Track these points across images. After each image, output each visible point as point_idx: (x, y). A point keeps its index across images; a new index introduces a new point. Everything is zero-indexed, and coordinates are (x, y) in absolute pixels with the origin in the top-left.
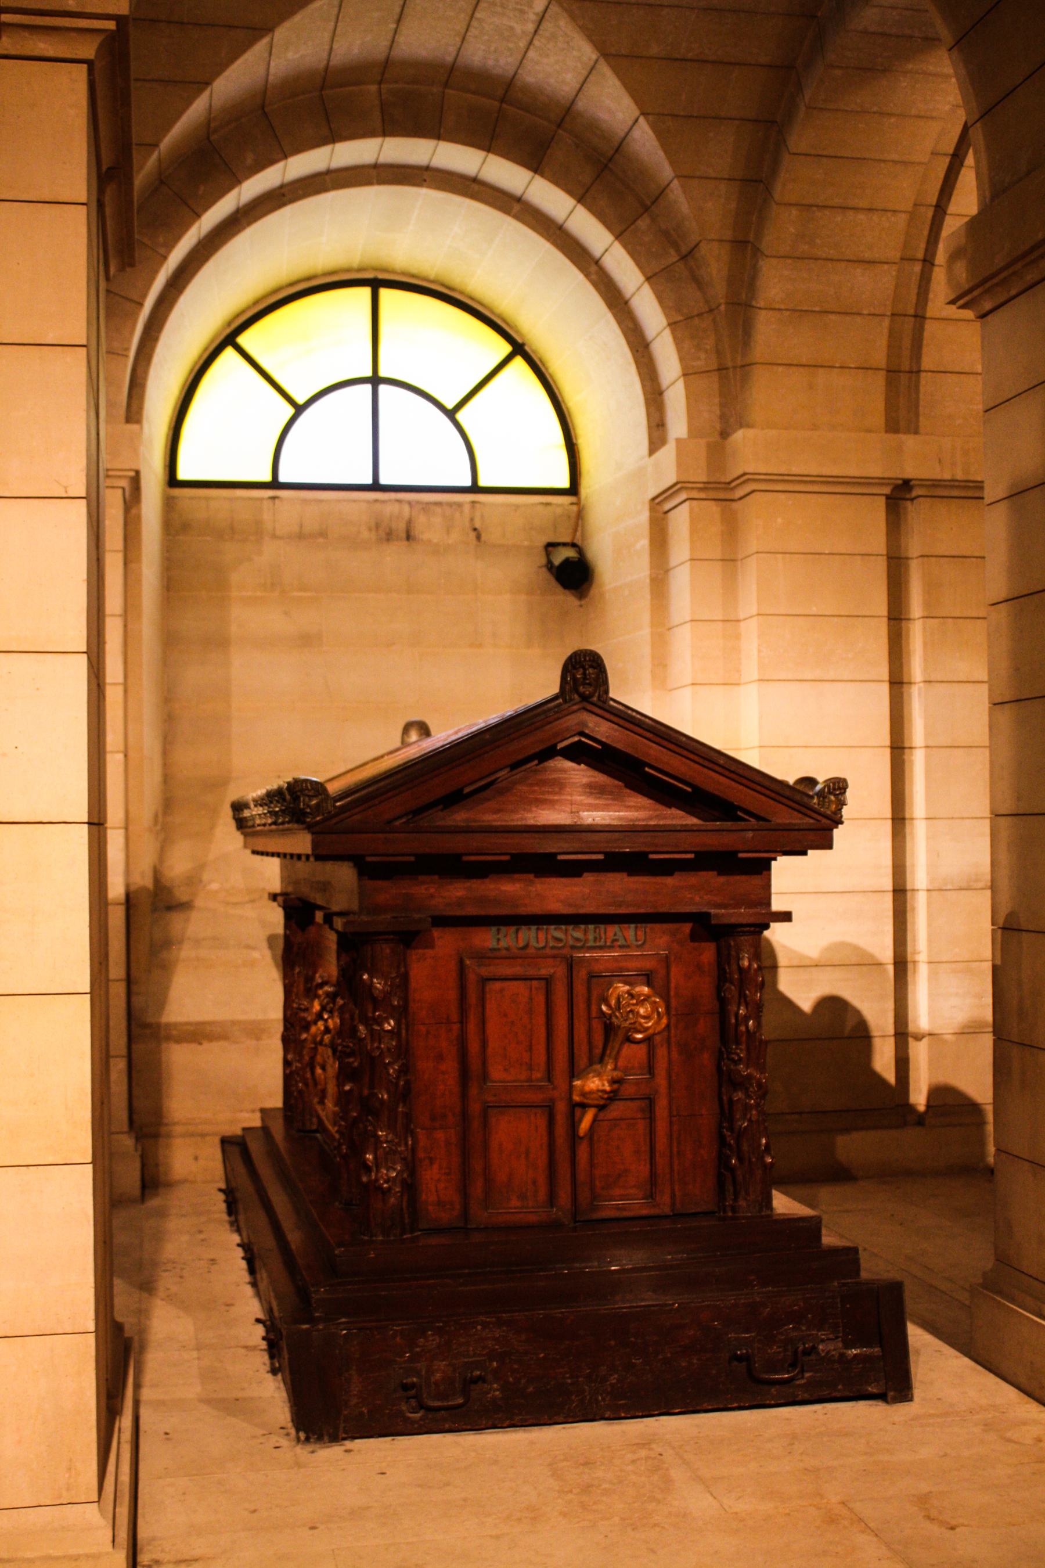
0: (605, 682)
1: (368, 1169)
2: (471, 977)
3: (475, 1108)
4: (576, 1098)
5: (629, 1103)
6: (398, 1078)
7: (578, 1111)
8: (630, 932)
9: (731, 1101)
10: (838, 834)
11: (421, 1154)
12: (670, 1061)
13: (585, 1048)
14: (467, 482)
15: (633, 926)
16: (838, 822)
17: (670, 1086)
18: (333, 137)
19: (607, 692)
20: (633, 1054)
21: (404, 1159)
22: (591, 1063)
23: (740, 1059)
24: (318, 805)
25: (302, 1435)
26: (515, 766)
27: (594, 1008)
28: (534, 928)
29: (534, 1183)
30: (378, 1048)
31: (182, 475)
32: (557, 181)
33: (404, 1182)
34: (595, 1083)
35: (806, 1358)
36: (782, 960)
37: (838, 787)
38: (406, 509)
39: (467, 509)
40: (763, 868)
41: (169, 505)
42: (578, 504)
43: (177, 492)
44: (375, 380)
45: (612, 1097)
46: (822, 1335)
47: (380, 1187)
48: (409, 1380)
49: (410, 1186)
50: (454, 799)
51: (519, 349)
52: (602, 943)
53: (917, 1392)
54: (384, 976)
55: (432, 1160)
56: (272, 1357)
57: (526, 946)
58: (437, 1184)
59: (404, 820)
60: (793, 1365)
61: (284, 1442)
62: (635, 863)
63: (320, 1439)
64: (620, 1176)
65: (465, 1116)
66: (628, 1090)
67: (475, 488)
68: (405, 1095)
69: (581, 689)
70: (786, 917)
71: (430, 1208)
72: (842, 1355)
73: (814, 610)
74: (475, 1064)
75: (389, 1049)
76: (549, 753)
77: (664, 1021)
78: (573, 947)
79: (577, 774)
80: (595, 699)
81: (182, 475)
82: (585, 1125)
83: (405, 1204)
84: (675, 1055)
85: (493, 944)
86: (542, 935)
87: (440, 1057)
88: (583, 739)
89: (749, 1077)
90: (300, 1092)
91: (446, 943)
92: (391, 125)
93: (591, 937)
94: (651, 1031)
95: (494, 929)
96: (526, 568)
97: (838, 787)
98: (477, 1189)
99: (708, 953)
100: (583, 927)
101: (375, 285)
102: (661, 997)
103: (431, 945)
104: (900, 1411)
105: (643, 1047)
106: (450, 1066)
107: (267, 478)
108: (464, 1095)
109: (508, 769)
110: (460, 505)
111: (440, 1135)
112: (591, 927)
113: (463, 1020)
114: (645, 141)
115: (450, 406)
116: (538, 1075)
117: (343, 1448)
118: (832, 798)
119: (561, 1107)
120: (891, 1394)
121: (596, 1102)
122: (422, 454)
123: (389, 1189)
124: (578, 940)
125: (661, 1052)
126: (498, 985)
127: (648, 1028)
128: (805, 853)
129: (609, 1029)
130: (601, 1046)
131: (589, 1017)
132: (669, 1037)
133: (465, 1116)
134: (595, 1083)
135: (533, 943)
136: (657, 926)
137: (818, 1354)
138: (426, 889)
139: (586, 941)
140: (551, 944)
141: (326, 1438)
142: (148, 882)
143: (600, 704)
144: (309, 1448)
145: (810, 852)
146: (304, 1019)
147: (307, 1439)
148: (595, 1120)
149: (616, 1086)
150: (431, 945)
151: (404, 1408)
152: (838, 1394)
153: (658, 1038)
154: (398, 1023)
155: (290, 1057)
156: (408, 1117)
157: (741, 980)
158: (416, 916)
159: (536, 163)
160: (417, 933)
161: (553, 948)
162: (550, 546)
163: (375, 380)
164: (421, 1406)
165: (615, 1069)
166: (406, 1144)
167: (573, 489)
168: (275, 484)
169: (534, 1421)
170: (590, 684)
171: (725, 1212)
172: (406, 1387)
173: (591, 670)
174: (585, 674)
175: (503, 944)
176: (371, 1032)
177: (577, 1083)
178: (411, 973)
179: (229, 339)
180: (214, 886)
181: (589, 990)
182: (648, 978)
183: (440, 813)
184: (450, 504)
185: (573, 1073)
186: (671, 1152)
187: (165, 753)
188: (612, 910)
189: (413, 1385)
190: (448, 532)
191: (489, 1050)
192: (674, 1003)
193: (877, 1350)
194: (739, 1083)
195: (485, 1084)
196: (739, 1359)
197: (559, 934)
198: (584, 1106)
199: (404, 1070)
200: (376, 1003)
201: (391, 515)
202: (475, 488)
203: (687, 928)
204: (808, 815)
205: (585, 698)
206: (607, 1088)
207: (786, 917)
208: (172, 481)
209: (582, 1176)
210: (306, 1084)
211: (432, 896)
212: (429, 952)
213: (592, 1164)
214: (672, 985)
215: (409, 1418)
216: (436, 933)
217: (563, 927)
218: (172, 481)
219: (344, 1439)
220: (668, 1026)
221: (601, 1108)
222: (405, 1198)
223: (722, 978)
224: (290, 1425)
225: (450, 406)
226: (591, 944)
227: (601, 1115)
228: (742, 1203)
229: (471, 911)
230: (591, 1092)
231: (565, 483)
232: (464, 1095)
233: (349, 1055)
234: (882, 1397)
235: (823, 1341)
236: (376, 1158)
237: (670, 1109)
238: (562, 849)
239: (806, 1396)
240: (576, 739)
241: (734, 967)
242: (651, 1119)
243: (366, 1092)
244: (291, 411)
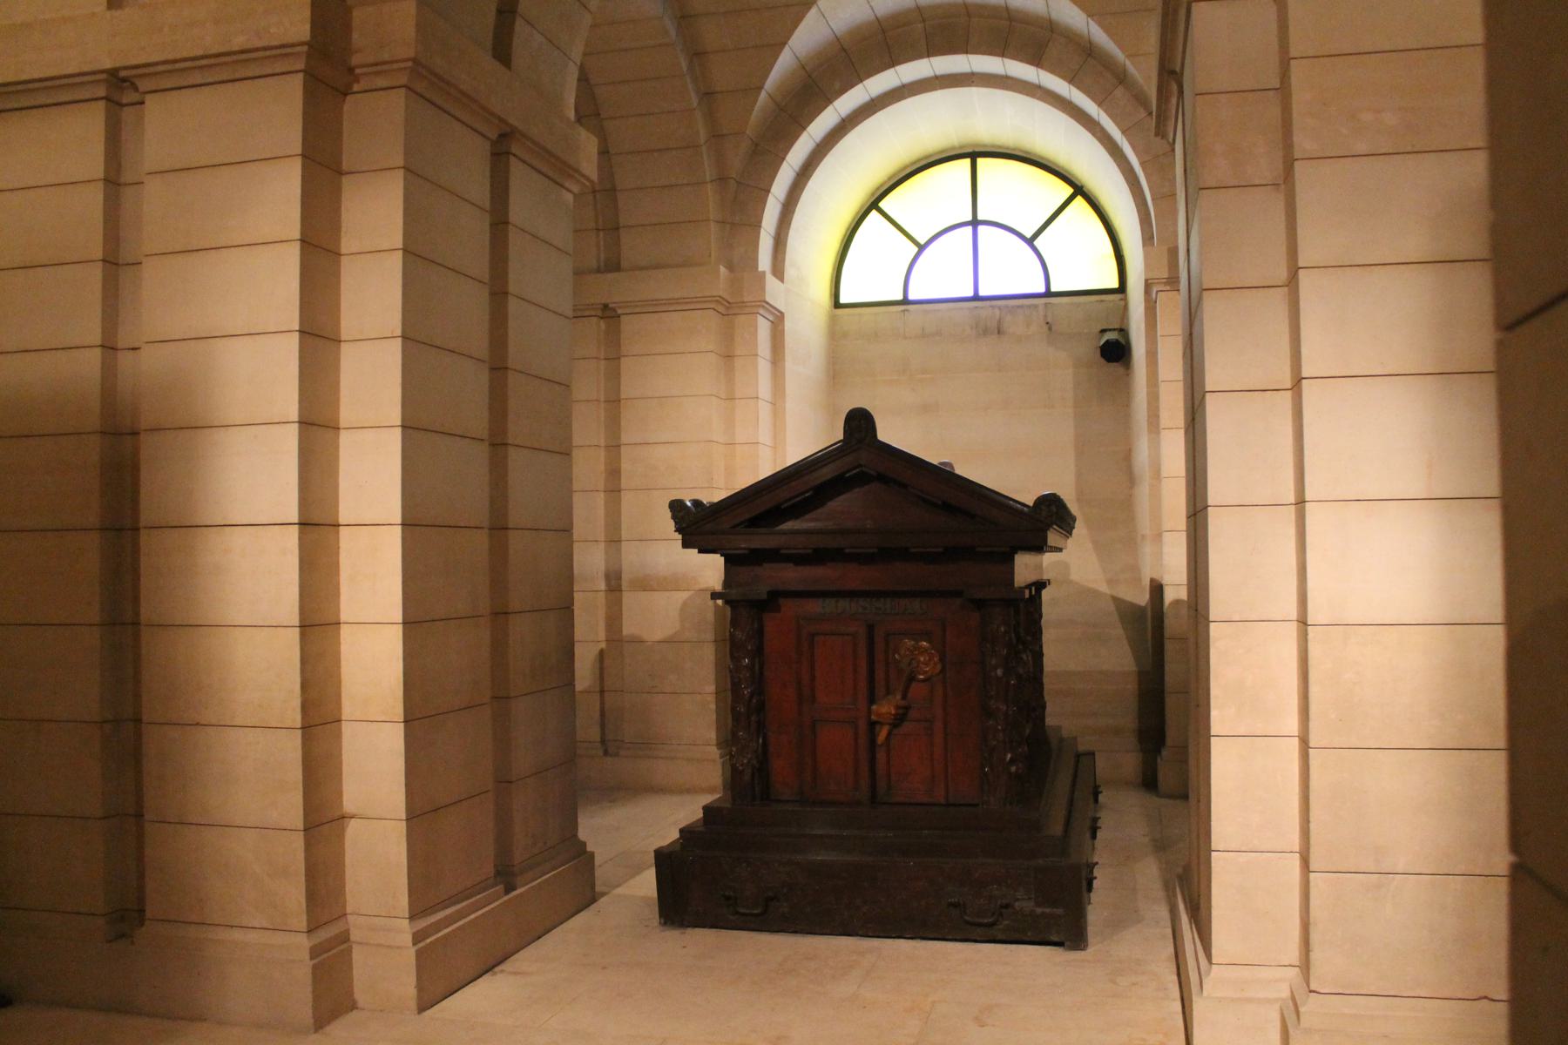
8: (916, 605)
14: (1042, 289)
18: (893, 63)
22: (888, 692)
31: (842, 300)
32: (1052, 72)
34: (885, 708)
38: (997, 312)
39: (1041, 308)
40: (1009, 559)
41: (833, 322)
42: (1125, 300)
43: (839, 311)
44: (975, 223)
45: (899, 719)
51: (1079, 190)
67: (1048, 293)
68: (761, 707)
77: (939, 667)
81: (842, 300)
82: (881, 737)
91: (789, 607)
92: (933, 49)
96: (1089, 349)
101: (973, 156)
103: (778, 610)
104: (1082, 954)
107: (900, 297)
110: (1036, 306)
114: (1099, 35)
115: (1029, 235)
119: (862, 725)
122: (1010, 273)
134: (885, 708)
148: (889, 734)
150: (778, 610)
159: (1036, 60)
162: (1103, 331)
163: (975, 223)
164: (737, 913)
165: (904, 697)
167: (1122, 288)
168: (905, 301)
172: (728, 898)
177: (874, 707)
179: (873, 204)
182: (927, 635)
184: (1029, 307)
185: (872, 700)
190: (1028, 326)
193: (1060, 911)
196: (955, 905)
198: (882, 724)
201: (988, 317)
202: (1048, 293)
208: (837, 305)
216: (782, 601)
218: (837, 305)
220: (943, 671)
225: (1029, 235)
229: (801, 588)
231: (1115, 285)
234: (1059, 944)
244: (916, 249)
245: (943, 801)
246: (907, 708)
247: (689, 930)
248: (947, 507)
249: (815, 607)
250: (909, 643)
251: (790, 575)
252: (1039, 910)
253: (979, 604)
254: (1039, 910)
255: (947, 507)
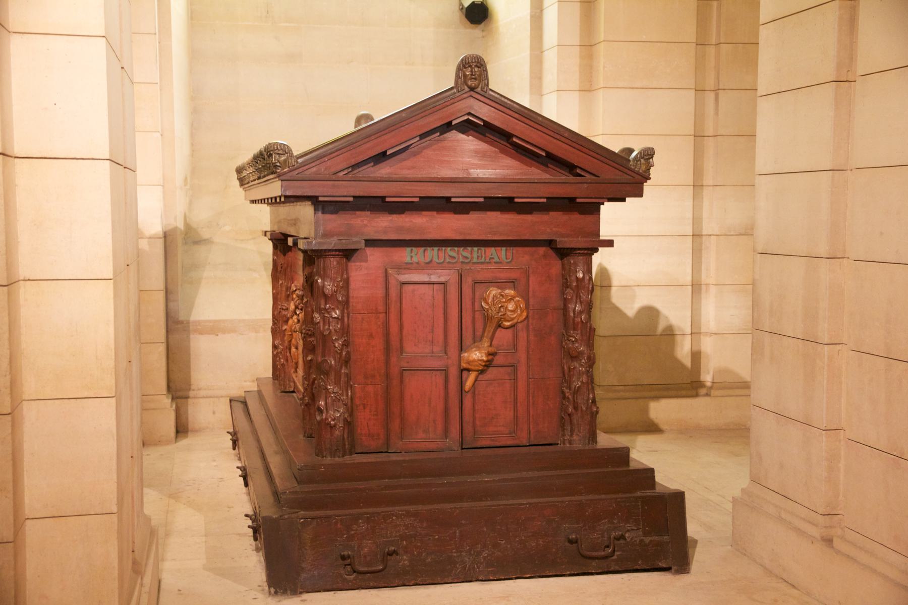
0: (487, 78)
1: (320, 411)
2: (393, 283)
3: (395, 371)
4: (464, 365)
5: (500, 369)
6: (342, 350)
7: (465, 373)
9: (569, 368)
10: (647, 187)
11: (357, 402)
12: (528, 341)
13: (470, 330)
15: (504, 249)
16: (648, 178)
17: (528, 359)
19: (487, 85)
20: (504, 336)
21: (346, 405)
23: (576, 340)
24: (285, 161)
25: (273, 590)
26: (423, 136)
27: (477, 304)
28: (436, 249)
29: (434, 421)
30: (329, 329)
33: (345, 420)
34: (477, 355)
35: (616, 542)
36: (615, 282)
37: (648, 155)
40: (593, 210)
45: (488, 364)
46: (628, 526)
47: (329, 424)
48: (346, 553)
49: (349, 424)
50: (382, 157)
52: (483, 260)
53: (695, 566)
54: (333, 280)
55: (364, 406)
56: (255, 539)
57: (431, 261)
58: (367, 421)
59: (346, 172)
60: (608, 547)
61: (260, 596)
62: (506, 204)
63: (285, 592)
64: (493, 418)
65: (388, 376)
66: (498, 360)
68: (347, 362)
69: (469, 83)
70: (610, 243)
71: (364, 438)
72: (641, 541)
73: (644, 38)
74: (395, 342)
75: (336, 331)
76: (448, 127)
77: (525, 314)
78: (462, 262)
79: (468, 143)
80: (479, 90)
82: (468, 384)
83: (346, 436)
84: (532, 338)
85: (408, 260)
86: (442, 254)
87: (371, 336)
88: (471, 118)
89: (582, 353)
90: (283, 365)
93: (475, 255)
94: (515, 321)
95: (408, 249)
97: (648, 155)
98: (396, 425)
99: (556, 266)
100: (469, 249)
102: (522, 297)
105: (510, 331)
106: (379, 343)
108: (387, 362)
109: (418, 138)
111: (370, 389)
112: (475, 249)
113: (387, 312)
116: (437, 349)
117: (300, 599)
118: (642, 161)
119: (454, 372)
120: (674, 568)
121: (477, 368)
123: (335, 425)
124: (466, 258)
125: (522, 335)
126: (411, 287)
127: (512, 319)
128: (623, 200)
129: (487, 318)
130: (481, 330)
131: (474, 311)
132: (528, 325)
133: (388, 376)
135: (436, 259)
136: (520, 249)
137: (625, 539)
138: (362, 221)
139: (472, 258)
140: (448, 260)
141: (289, 592)
142: (181, 225)
143: (482, 93)
144: (276, 599)
145: (627, 199)
146: (285, 316)
147: (276, 593)
148: (476, 380)
149: (490, 357)
151: (342, 572)
152: (638, 567)
153: (520, 325)
154: (342, 313)
155: (276, 342)
156: (348, 376)
157: (577, 286)
158: (355, 239)
160: (355, 250)
161: (449, 263)
164: (355, 572)
166: (347, 395)
169: (431, 581)
170: (475, 79)
171: (564, 444)
172: (343, 558)
173: (476, 69)
174: (473, 72)
175: (415, 259)
176: (324, 318)
178: (351, 279)
180: (227, 228)
181: (474, 293)
182: (512, 283)
183: (372, 169)
186: (528, 401)
187: (192, 135)
188: (490, 237)
189: (349, 557)
191: (405, 332)
192: (531, 300)
194: (575, 357)
195: (401, 354)
197: (453, 254)
198: (468, 370)
199: (346, 344)
200: (326, 298)
203: (542, 250)
204: (627, 176)
205: (472, 89)
206: (485, 358)
207: (610, 243)
209: (467, 417)
210: (287, 361)
211: (366, 226)
212: (363, 264)
213: (474, 410)
214: (531, 289)
215: (346, 579)
216: (369, 251)
217: (456, 249)
219: (301, 593)
220: (527, 317)
221: (482, 372)
222: (346, 431)
223: (566, 285)
224: (265, 584)
226: (475, 260)
227: (481, 376)
228: (575, 437)
230: (474, 361)
232: (387, 362)
233: (310, 336)
235: (628, 531)
236: (326, 404)
237: (528, 375)
238: (455, 193)
239: (617, 568)
240: (466, 118)
241: (573, 278)
242: (516, 380)
243: (320, 359)
245: (525, 442)
246: (493, 354)
247: (305, 596)
248: (551, 160)
249: (408, 255)
250: (494, 292)
251: (382, 225)
252: (647, 540)
253: (563, 253)
254: (647, 540)
255: (551, 160)
